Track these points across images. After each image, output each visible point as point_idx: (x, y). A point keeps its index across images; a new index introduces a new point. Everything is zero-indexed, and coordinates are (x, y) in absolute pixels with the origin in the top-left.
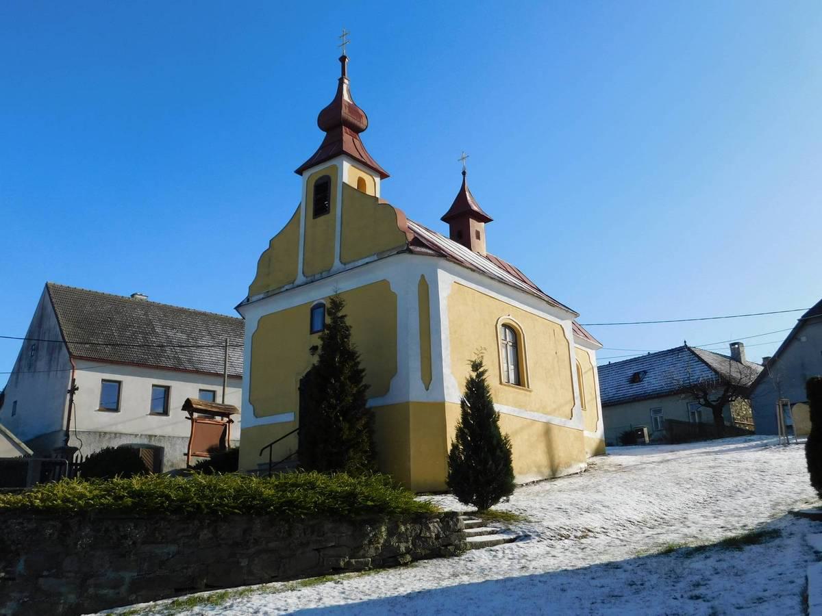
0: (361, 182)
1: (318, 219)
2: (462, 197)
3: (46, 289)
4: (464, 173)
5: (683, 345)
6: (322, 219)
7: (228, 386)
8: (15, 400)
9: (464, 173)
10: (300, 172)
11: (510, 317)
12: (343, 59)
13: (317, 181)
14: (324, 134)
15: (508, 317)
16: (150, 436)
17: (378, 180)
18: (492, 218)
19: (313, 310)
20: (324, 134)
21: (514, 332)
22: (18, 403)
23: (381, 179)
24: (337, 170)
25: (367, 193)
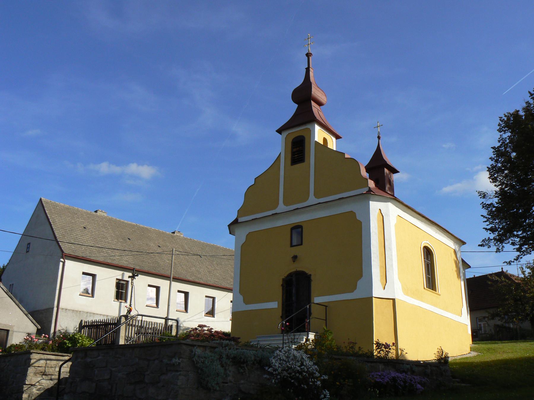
0: (325, 140)
1: (294, 166)
2: (378, 153)
3: (40, 202)
4: (379, 138)
5: (501, 270)
6: (298, 166)
7: (172, 281)
8: (11, 283)
9: (379, 138)
10: (280, 131)
11: (428, 242)
12: (308, 55)
13: (293, 140)
14: (296, 106)
15: (427, 242)
16: (26, 315)
17: (334, 139)
18: (399, 171)
19: (292, 229)
20: (296, 106)
21: (428, 253)
22: (14, 285)
23: (336, 139)
24: (311, 133)
25: (328, 147)
